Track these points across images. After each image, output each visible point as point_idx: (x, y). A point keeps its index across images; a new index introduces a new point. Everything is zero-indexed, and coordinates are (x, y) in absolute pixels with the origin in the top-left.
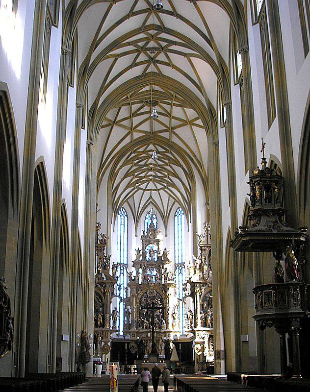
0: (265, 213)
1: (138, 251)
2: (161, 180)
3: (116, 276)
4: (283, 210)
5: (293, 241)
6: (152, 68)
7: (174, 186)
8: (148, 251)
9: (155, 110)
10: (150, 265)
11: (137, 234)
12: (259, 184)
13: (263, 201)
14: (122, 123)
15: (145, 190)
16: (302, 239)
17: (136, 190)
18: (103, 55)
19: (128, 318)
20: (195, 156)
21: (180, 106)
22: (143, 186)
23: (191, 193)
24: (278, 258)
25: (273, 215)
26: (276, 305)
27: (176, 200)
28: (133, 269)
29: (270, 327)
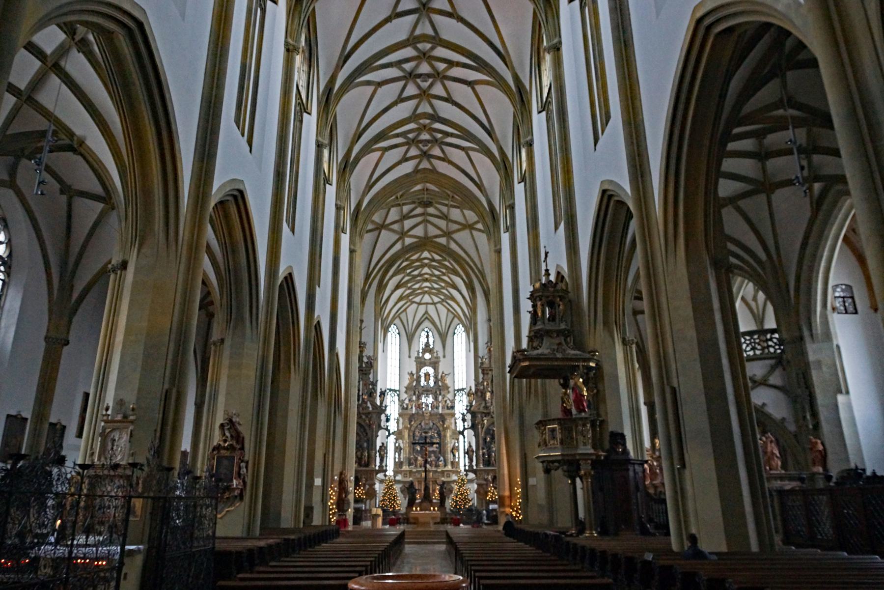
0: (548, 333)
1: (411, 374)
2: (439, 292)
3: (384, 405)
4: (568, 330)
5: (581, 367)
6: (425, 165)
7: (453, 299)
8: (423, 375)
9: (431, 210)
10: (427, 391)
11: (412, 355)
12: (541, 300)
13: (546, 321)
14: (393, 227)
15: (419, 304)
16: (592, 364)
17: (409, 303)
18: (367, 150)
19: (399, 455)
20: (475, 265)
21: (458, 207)
22: (417, 299)
23: (473, 310)
24: (565, 386)
25: (558, 336)
26: (562, 443)
27: (456, 316)
28: (405, 396)
29: (556, 470)
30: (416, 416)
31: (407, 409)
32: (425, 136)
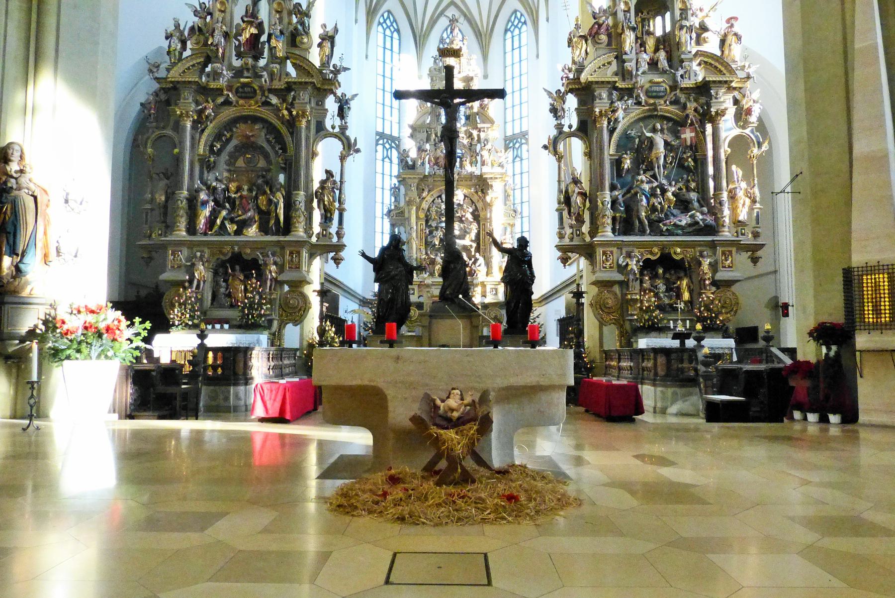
30: (430, 180)
31: (413, 167)
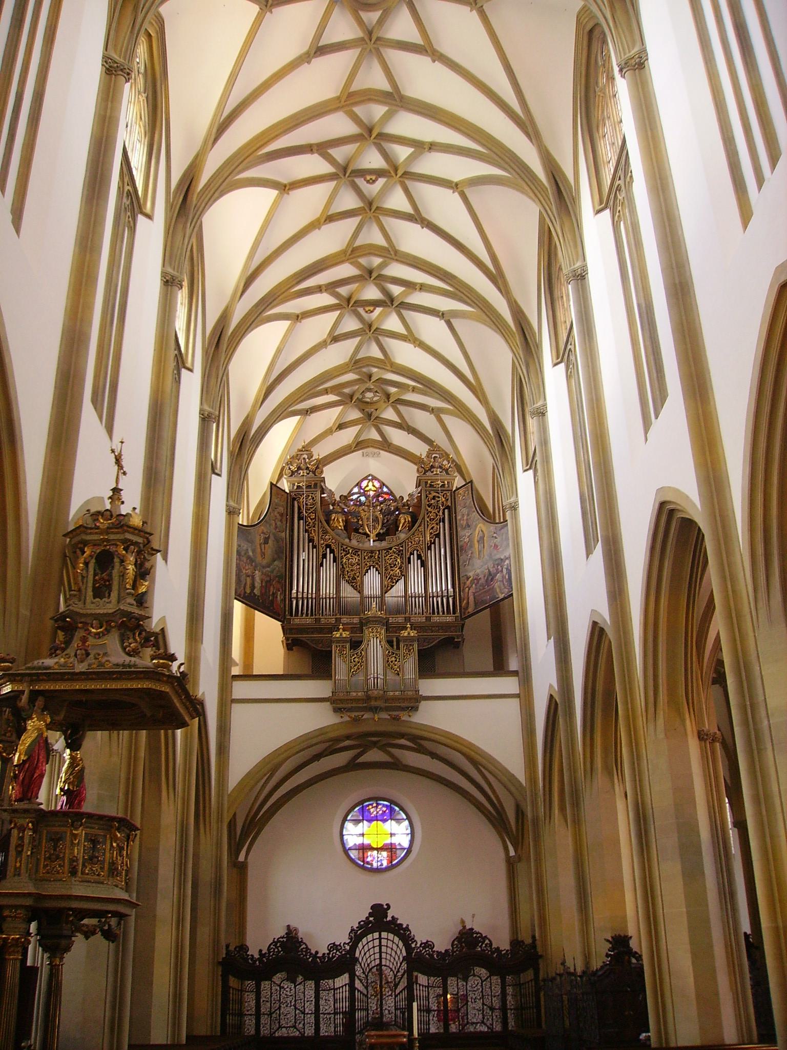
32: (372, 293)
